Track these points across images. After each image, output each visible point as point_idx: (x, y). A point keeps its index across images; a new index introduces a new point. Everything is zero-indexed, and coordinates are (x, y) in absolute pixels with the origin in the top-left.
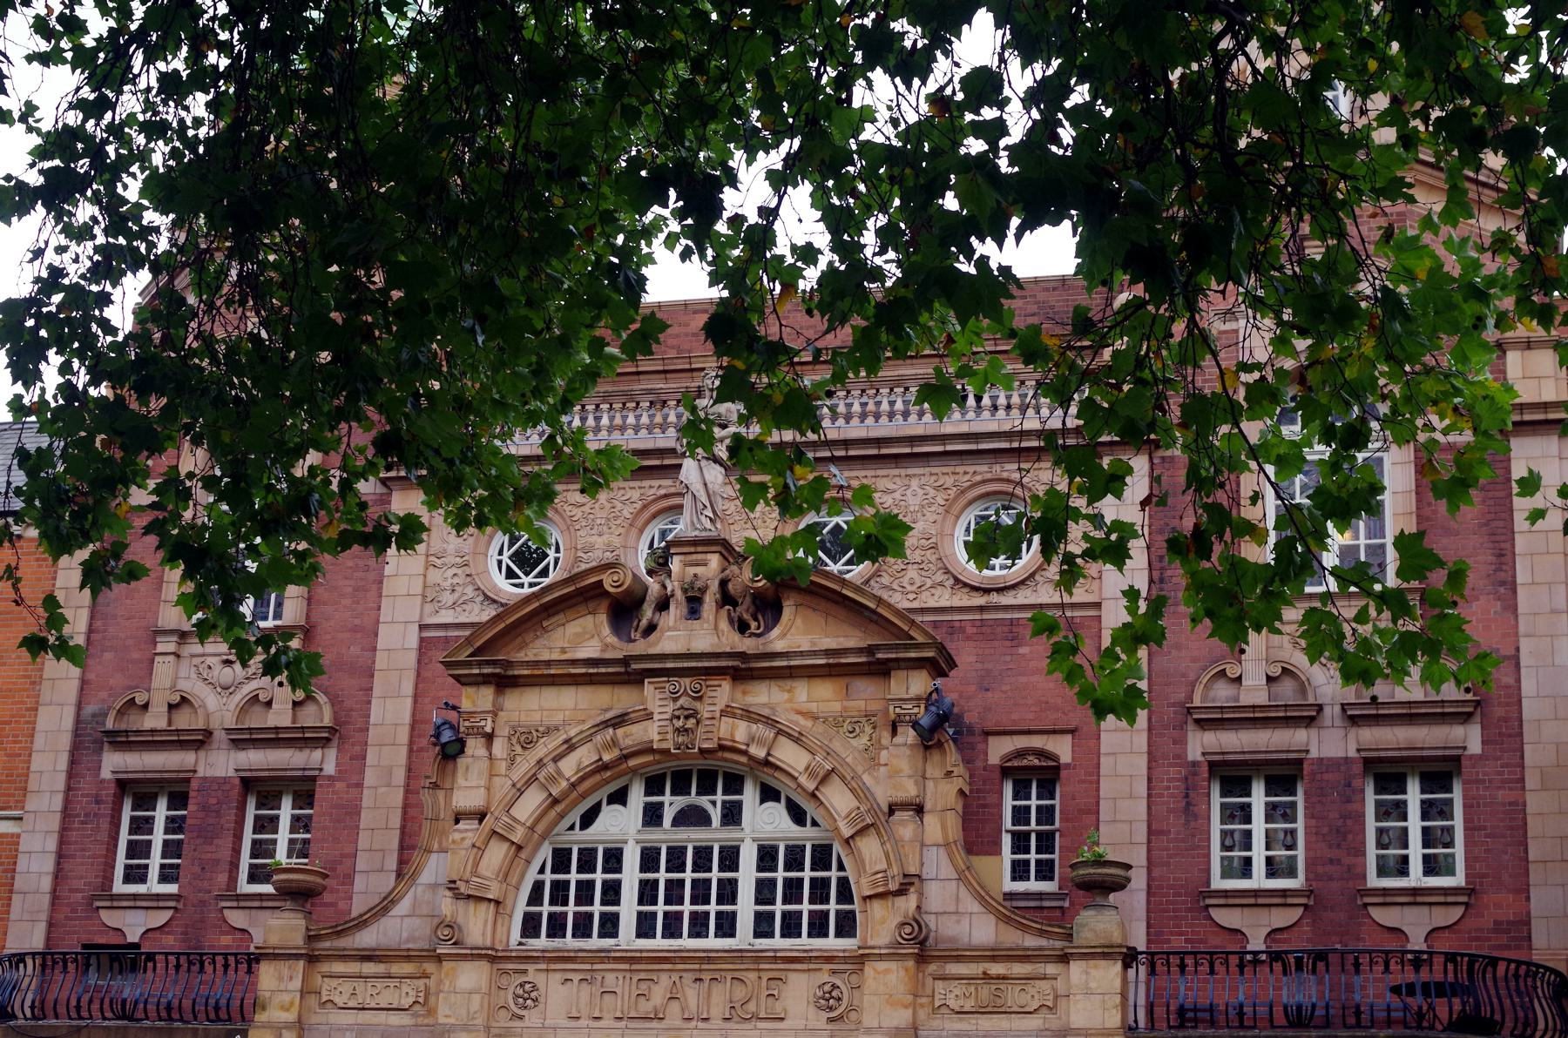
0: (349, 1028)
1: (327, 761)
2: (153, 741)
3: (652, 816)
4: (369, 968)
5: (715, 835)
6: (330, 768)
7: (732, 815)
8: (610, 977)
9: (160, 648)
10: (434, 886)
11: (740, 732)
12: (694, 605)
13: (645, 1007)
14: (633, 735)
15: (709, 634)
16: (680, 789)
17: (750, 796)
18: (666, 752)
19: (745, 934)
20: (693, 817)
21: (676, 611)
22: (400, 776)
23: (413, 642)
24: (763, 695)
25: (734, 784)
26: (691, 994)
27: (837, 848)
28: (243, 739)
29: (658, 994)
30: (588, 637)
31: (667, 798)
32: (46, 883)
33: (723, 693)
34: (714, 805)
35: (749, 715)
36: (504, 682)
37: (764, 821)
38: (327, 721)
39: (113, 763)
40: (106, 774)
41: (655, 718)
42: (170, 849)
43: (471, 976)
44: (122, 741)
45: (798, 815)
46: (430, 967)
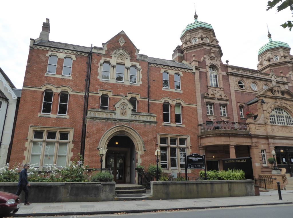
0: (259, 132)
1: (228, 103)
2: (211, 98)
3: (276, 112)
4: (259, 125)
5: (281, 114)
6: (228, 104)
7: (283, 113)
8: (279, 128)
9: (209, 88)
10: (263, 117)
11: (285, 105)
12: (278, 92)
13: (283, 131)
14: (277, 104)
15: (280, 95)
16: (278, 110)
17: (283, 111)
18: (280, 106)
19: (286, 125)
20: (279, 113)
21: (277, 92)
22: (236, 105)
23: (234, 91)
24: (285, 102)
25: (282, 110)
26: (286, 130)
27: (291, 117)
28: (218, 99)
29: (283, 129)
30: (269, 94)
31: (277, 111)
32: (201, 113)
33: (284, 101)
34: (281, 111)
35: (286, 104)
36: (265, 97)
37: (285, 114)
38: (228, 99)
39: (206, 100)
40: (205, 101)
41: (279, 103)
42: (208, 110)
43: (269, 127)
44: (206, 98)
45: (287, 113)
46: (264, 126)
